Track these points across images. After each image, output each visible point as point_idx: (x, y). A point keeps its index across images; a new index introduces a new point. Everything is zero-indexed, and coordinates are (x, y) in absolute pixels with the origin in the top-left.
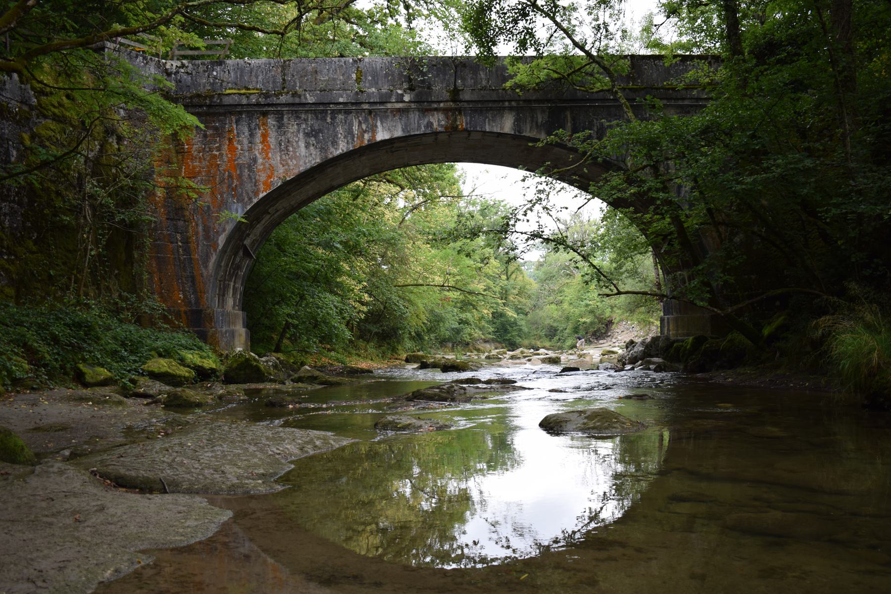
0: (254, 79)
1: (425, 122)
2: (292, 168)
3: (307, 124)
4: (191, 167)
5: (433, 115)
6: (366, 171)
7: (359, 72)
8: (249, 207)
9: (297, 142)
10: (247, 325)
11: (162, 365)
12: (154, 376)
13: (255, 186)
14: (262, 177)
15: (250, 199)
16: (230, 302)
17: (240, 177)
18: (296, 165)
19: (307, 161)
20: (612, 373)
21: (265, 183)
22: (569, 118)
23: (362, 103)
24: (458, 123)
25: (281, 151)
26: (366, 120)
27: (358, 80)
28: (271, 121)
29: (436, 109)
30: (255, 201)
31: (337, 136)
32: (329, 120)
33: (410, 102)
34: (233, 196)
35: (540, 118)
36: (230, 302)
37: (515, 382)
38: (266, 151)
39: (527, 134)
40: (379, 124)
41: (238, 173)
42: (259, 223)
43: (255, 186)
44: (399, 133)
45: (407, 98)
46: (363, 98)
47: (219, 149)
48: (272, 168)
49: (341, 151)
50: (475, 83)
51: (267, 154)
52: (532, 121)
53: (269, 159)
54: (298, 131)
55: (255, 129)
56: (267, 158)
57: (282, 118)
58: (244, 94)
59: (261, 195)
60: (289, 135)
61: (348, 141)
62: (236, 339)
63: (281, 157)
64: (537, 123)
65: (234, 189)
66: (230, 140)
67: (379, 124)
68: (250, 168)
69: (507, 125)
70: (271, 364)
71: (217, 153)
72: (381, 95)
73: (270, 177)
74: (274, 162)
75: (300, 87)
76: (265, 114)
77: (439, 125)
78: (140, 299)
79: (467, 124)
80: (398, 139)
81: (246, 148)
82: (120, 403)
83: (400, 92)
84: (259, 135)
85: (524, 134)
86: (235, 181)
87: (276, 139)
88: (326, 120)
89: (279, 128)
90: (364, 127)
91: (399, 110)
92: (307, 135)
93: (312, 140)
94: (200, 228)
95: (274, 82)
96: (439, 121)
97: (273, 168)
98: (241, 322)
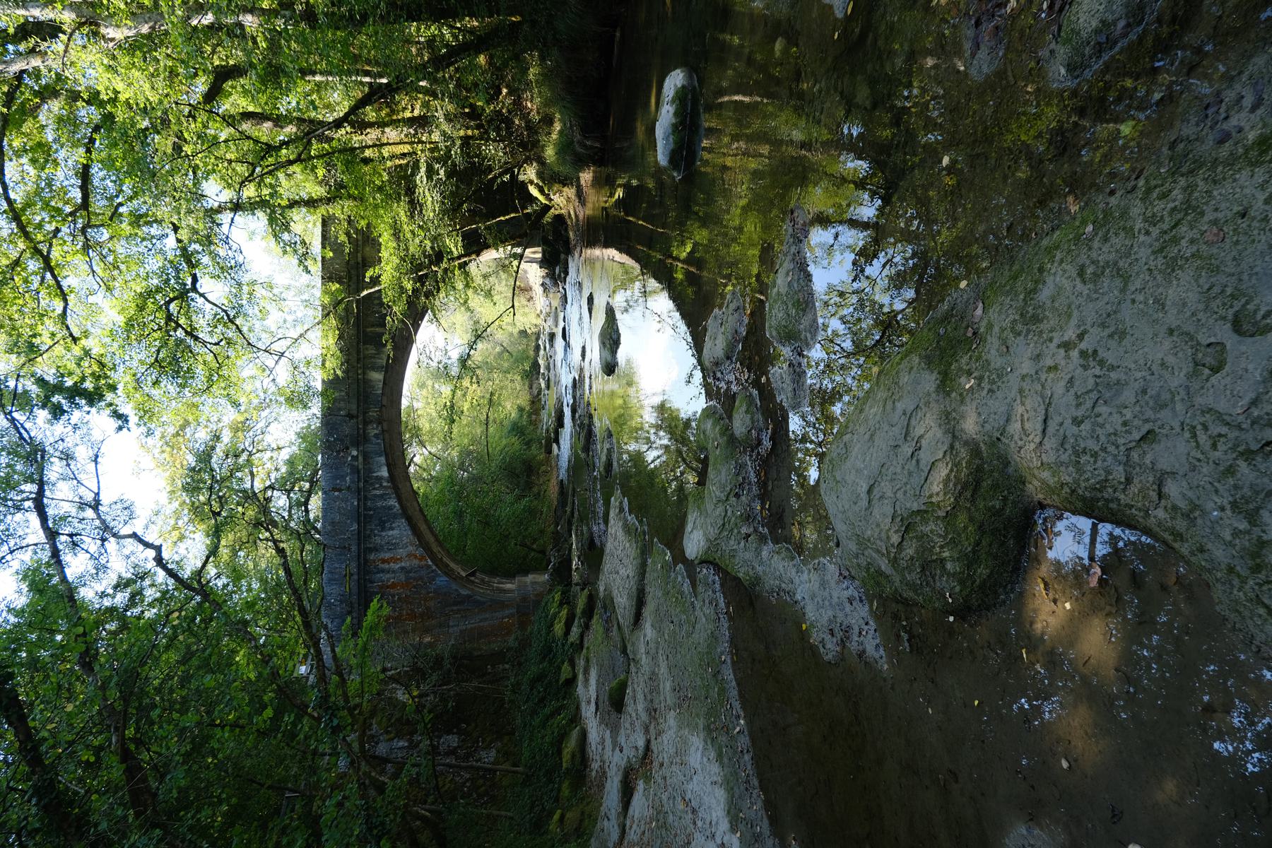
6: (408, 484)
7: (334, 489)
11: (559, 628)
12: (567, 632)
14: (416, 562)
15: (433, 571)
16: (509, 586)
17: (415, 579)
20: (568, 306)
25: (395, 549)
26: (372, 484)
27: (340, 490)
28: (372, 557)
30: (434, 567)
35: (371, 350)
36: (509, 586)
37: (575, 379)
38: (395, 560)
44: (383, 459)
45: (355, 453)
46: (354, 487)
47: (393, 596)
48: (409, 555)
50: (344, 400)
56: (401, 560)
59: (430, 563)
66: (388, 587)
69: (377, 376)
73: (416, 557)
76: (366, 561)
78: (509, 649)
80: (387, 460)
82: (588, 648)
91: (364, 459)
92: (383, 529)
94: (455, 608)
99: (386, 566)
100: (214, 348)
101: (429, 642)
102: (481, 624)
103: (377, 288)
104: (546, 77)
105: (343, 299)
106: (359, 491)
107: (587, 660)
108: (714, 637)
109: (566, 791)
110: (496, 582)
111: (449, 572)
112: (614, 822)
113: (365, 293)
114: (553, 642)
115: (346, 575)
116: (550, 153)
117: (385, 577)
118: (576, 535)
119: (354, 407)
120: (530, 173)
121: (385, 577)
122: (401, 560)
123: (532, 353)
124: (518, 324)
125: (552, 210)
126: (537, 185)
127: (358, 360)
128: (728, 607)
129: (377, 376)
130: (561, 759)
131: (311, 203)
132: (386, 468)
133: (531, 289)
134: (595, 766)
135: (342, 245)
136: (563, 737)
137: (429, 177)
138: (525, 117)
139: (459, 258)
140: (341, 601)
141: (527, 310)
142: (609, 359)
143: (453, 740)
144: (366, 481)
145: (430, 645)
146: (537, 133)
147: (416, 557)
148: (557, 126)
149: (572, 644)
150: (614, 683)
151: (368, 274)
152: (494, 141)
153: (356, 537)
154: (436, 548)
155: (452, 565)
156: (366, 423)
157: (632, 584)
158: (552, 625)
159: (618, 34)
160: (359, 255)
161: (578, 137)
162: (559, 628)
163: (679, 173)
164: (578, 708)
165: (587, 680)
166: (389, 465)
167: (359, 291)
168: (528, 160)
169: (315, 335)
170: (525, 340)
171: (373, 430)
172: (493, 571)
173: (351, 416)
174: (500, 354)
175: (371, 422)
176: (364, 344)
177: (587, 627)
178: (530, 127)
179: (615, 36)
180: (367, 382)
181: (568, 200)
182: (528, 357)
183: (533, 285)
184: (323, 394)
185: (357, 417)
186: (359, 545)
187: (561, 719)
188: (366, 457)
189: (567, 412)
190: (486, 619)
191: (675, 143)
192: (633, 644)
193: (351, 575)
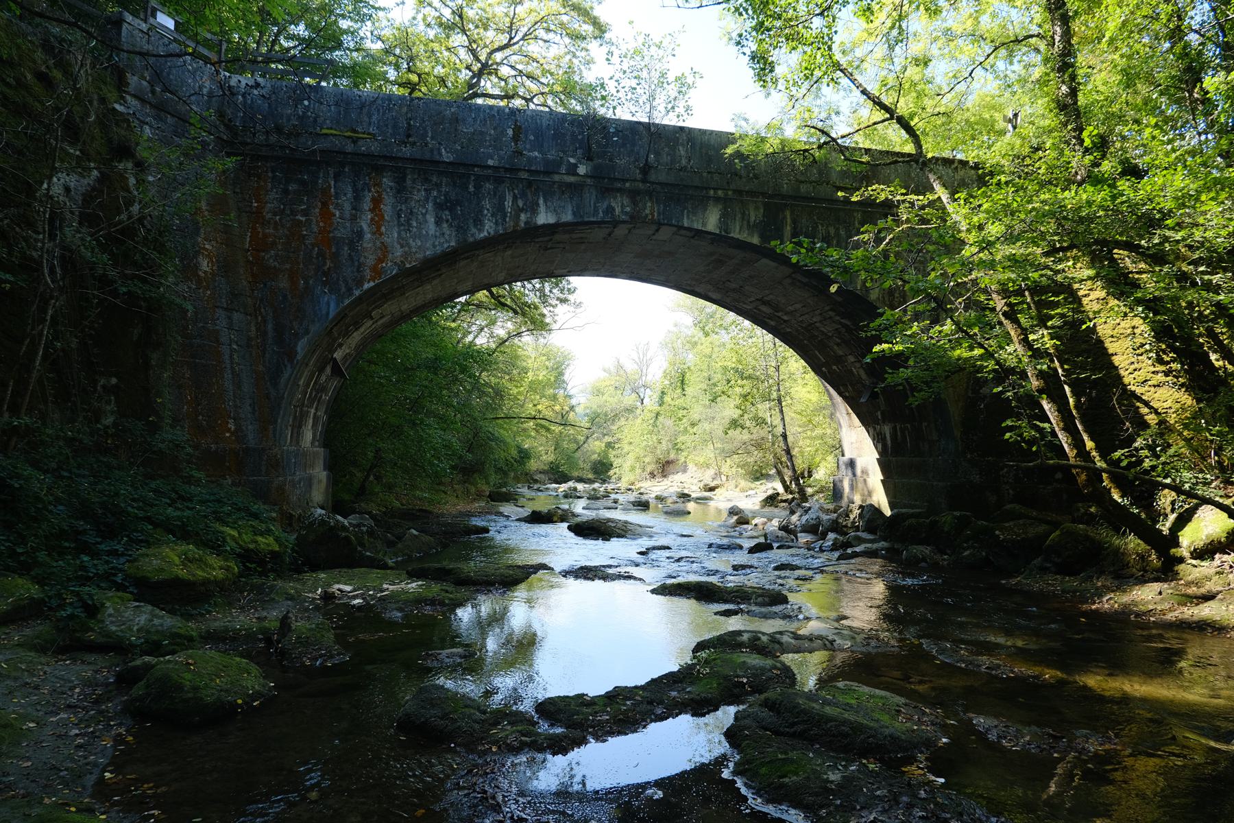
0: (366, 119)
1: (605, 206)
2: (414, 250)
3: (439, 191)
4: (260, 235)
5: (615, 198)
7: (518, 130)
8: (347, 302)
9: (424, 215)
10: (331, 466)
13: (358, 271)
14: (370, 260)
15: (350, 290)
16: (308, 435)
18: (419, 247)
19: (437, 243)
22: (789, 221)
23: (519, 170)
24: (647, 211)
25: (400, 224)
26: (523, 195)
27: (516, 138)
28: (387, 181)
29: (619, 190)
30: (357, 293)
31: (481, 211)
32: (471, 189)
33: (586, 176)
34: (324, 284)
35: (755, 215)
36: (308, 435)
38: (377, 223)
39: (735, 235)
40: (541, 201)
41: (334, 250)
42: (356, 329)
43: (358, 271)
44: (568, 217)
45: (582, 170)
47: (306, 213)
48: (385, 249)
49: (486, 233)
51: (379, 228)
52: (743, 219)
53: (381, 234)
54: (427, 199)
55: (363, 190)
56: (377, 232)
57: (404, 179)
58: (349, 137)
59: (366, 286)
60: (413, 204)
61: (496, 221)
62: (315, 487)
63: (399, 234)
64: (749, 222)
65: (325, 274)
67: (541, 201)
70: (364, 529)
71: (303, 219)
73: (380, 260)
74: (389, 240)
75: (432, 138)
76: (379, 170)
77: (622, 211)
79: (659, 214)
81: (347, 215)
83: (572, 160)
84: (368, 199)
85: (732, 235)
86: (328, 262)
87: (394, 207)
88: (467, 188)
89: (399, 192)
90: (520, 203)
91: (569, 185)
92: (439, 207)
93: (446, 214)
94: (270, 326)
95: (395, 126)
96: (623, 206)
97: (386, 248)
98: (321, 463)
99: (367, 204)
101: (197, 267)
102: (228, 375)
106: (513, 170)
111: (345, 323)
115: (354, 131)
117: (346, 202)
118: (419, 601)
119: (662, 177)
121: (346, 202)
122: (377, 232)
123: (575, 474)
127: (739, 192)
132: (551, 220)
133: (665, 476)
140: (302, 118)
141: (638, 471)
147: (380, 260)
153: (427, 156)
155: (357, 337)
156: (634, 195)
158: (183, 533)
170: (588, 467)
171: (620, 206)
172: (338, 413)
173: (646, 169)
174: (576, 441)
175: (634, 203)
176: (766, 205)
183: (671, 478)
185: (644, 181)
186: (413, 160)
188: (575, 190)
193: (355, 141)
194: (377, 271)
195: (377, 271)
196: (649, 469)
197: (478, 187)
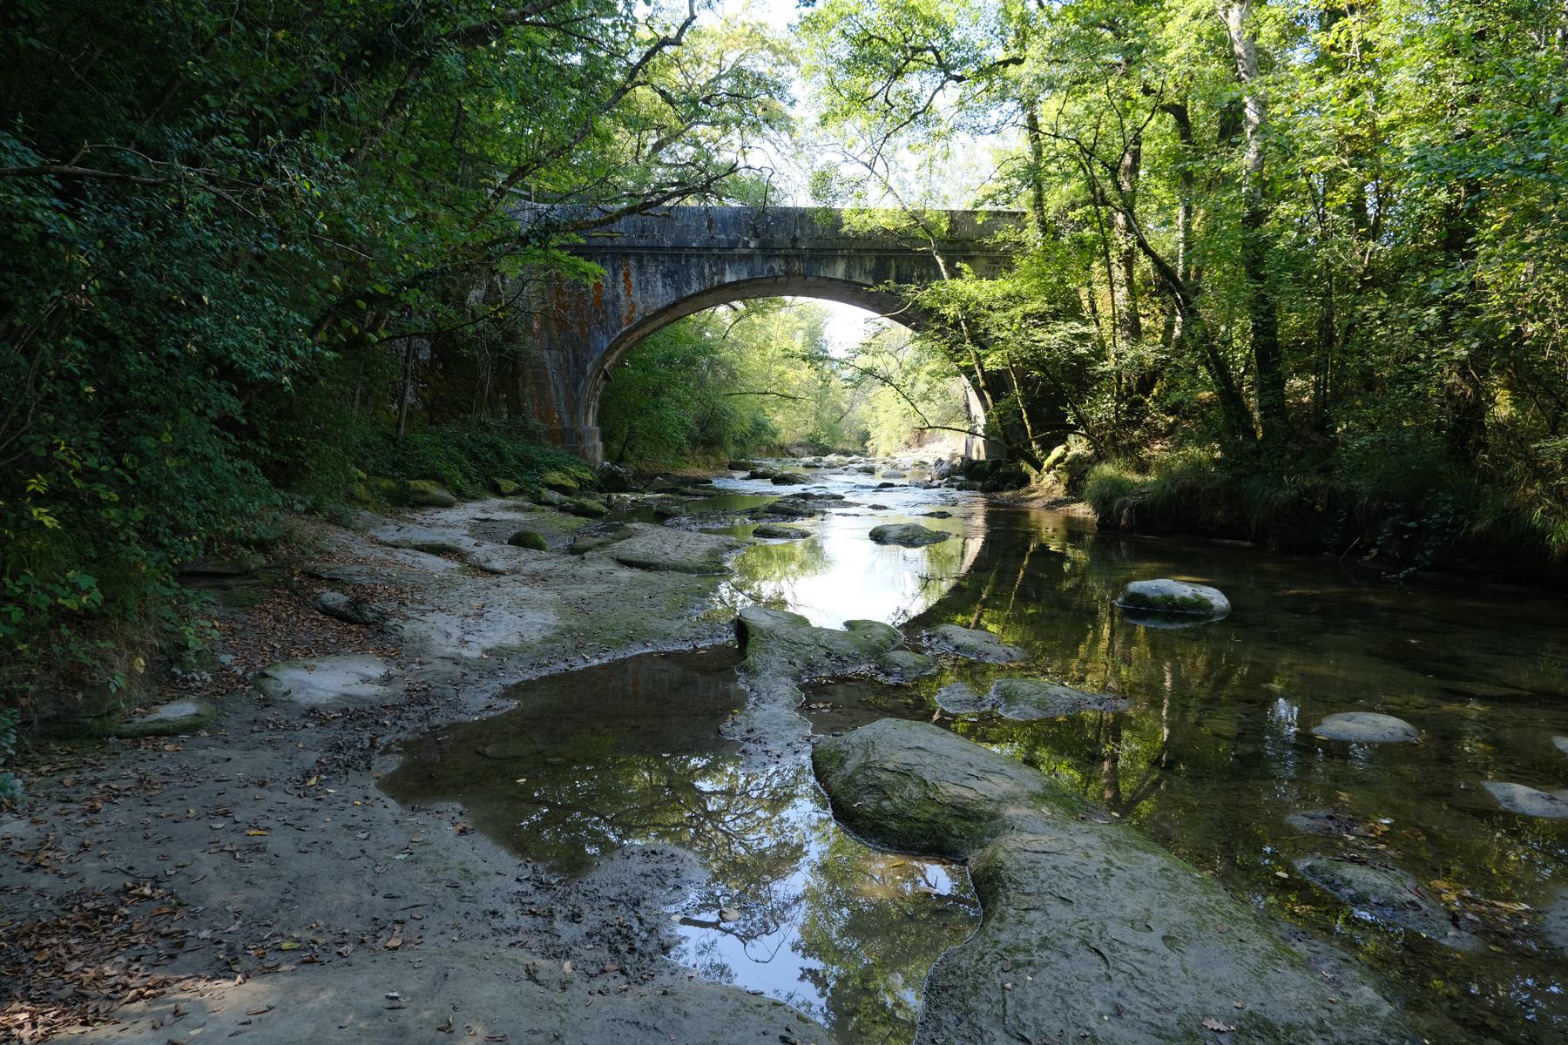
7: (710, 221)
11: (555, 477)
14: (625, 312)
17: (605, 312)
20: (921, 490)
21: (628, 318)
26: (716, 264)
27: (709, 227)
28: (632, 262)
30: (619, 333)
35: (870, 265)
38: (628, 288)
44: (744, 276)
45: (752, 245)
48: (633, 305)
50: (812, 233)
56: (628, 295)
59: (624, 329)
68: (614, 304)
72: (730, 241)
73: (631, 312)
76: (627, 255)
80: (744, 281)
91: (745, 255)
92: (664, 276)
93: (669, 281)
99: (621, 278)
100: (880, 99)
103: (945, 274)
104: (1197, 466)
105: (932, 235)
106: (708, 248)
107: (530, 510)
108: (666, 637)
109: (386, 484)
110: (594, 404)
111: (610, 350)
112: (398, 537)
113: (940, 261)
114: (539, 471)
116: (1107, 470)
118: (662, 499)
120: (1078, 446)
122: (628, 295)
123: (840, 446)
124: (877, 430)
125: (1035, 472)
126: (1065, 455)
127: (858, 250)
128: (702, 649)
129: (839, 271)
130: (417, 479)
131: (1039, 202)
132: (734, 280)
133: (921, 446)
134: (418, 517)
135: (990, 234)
136: (442, 481)
137: (1077, 336)
138: (1144, 442)
139: (981, 366)
141: (895, 441)
142: (892, 535)
143: (425, 354)
144: (720, 257)
145: (529, 328)
146: (1127, 455)
147: (631, 312)
148: (1137, 478)
149: (540, 492)
150: (541, 538)
151: (965, 267)
152: (1116, 408)
153: (655, 244)
154: (636, 335)
155: (617, 353)
156: (787, 258)
157: (661, 559)
159: (1248, 544)
160: (977, 253)
161: (1131, 501)
162: (555, 477)
163: (1123, 603)
164: (474, 498)
165: (508, 509)
166: (737, 283)
167: (941, 252)
168: (1094, 443)
169: (890, 203)
170: (855, 438)
171: (778, 266)
172: (604, 402)
173: (795, 240)
174: (841, 410)
175: (788, 264)
177: (563, 509)
178: (1132, 448)
179: (1245, 540)
180: (833, 259)
181: (1050, 490)
182: (834, 441)
183: (927, 447)
184: (828, 211)
185: (793, 248)
186: (647, 248)
187: (459, 480)
188: (748, 258)
189: (797, 489)
190: (558, 393)
191: (1153, 599)
192: (600, 558)
193: (612, 238)
194: (630, 320)
195: (630, 320)
196: (905, 438)
197: (687, 261)
